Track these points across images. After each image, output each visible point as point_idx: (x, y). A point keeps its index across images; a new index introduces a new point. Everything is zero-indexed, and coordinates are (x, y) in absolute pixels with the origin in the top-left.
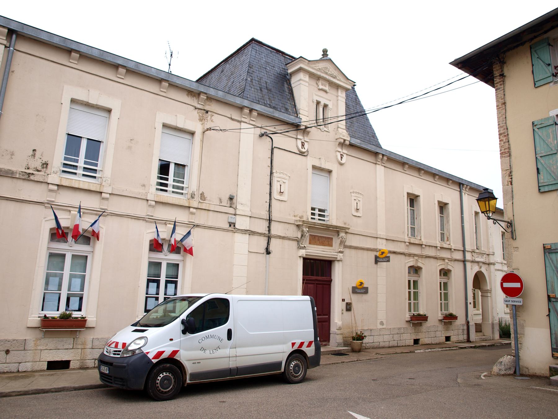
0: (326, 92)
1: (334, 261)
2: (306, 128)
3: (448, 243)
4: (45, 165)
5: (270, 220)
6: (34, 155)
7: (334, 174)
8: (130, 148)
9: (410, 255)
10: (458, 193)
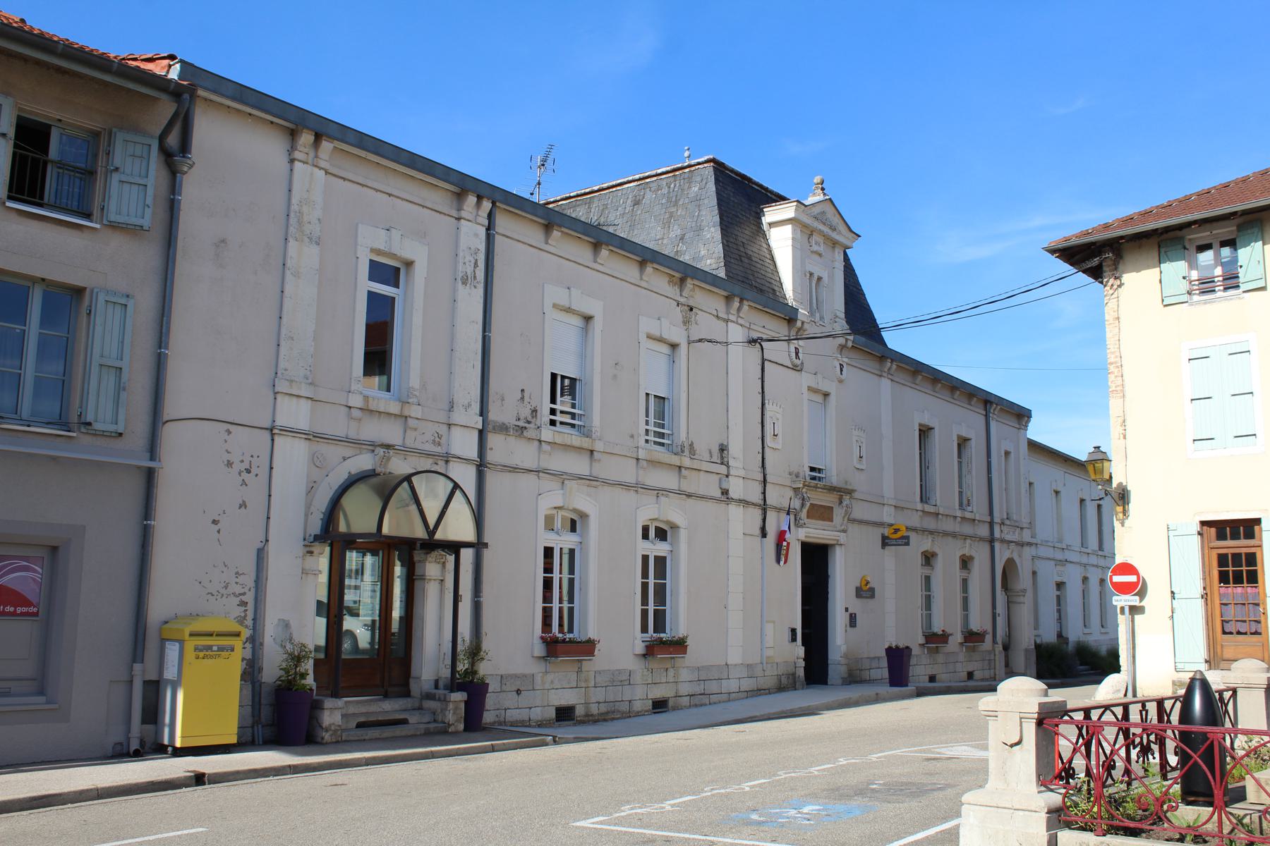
1: (833, 545)
3: (969, 509)
4: (534, 411)
6: (522, 398)
7: (832, 398)
8: (615, 377)
10: (982, 419)
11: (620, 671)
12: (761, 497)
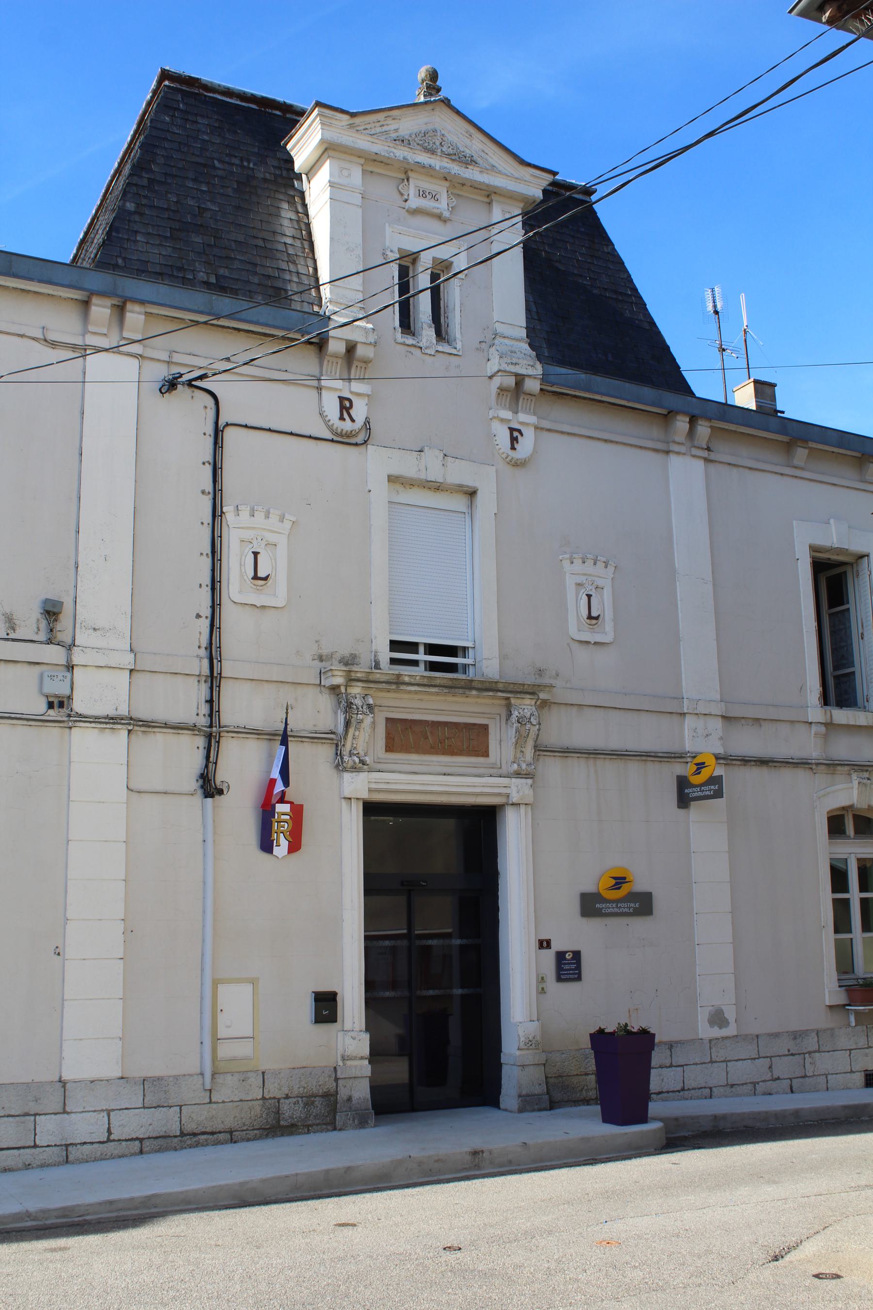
0: (439, 217)
1: (502, 806)
5: (214, 679)
7: (486, 501)
9: (832, 765)
12: (204, 709)
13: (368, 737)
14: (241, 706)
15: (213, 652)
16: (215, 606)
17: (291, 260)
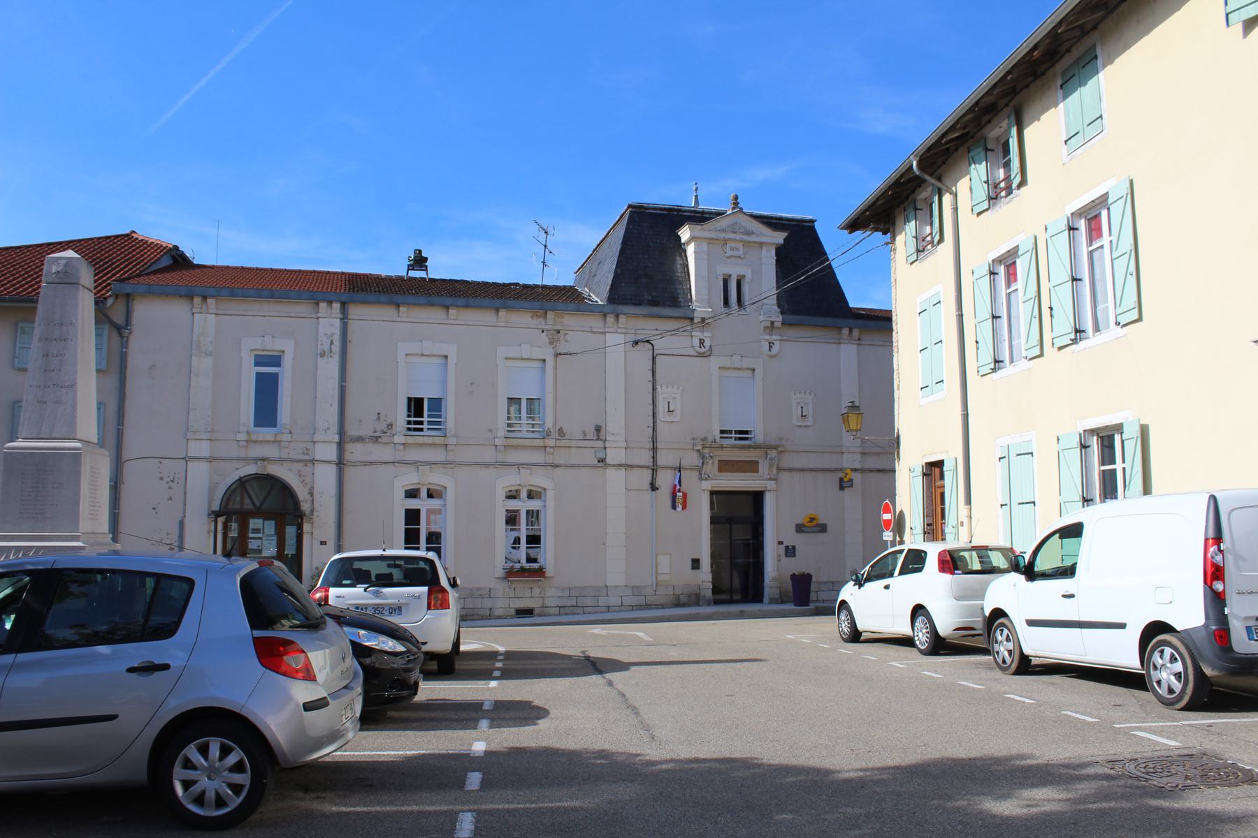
2: (703, 320)
4: (390, 426)
5: (654, 449)
6: (379, 418)
7: (759, 372)
11: (479, 589)
13: (711, 468)
14: (664, 458)
15: (654, 440)
16: (654, 423)
17: (681, 283)
